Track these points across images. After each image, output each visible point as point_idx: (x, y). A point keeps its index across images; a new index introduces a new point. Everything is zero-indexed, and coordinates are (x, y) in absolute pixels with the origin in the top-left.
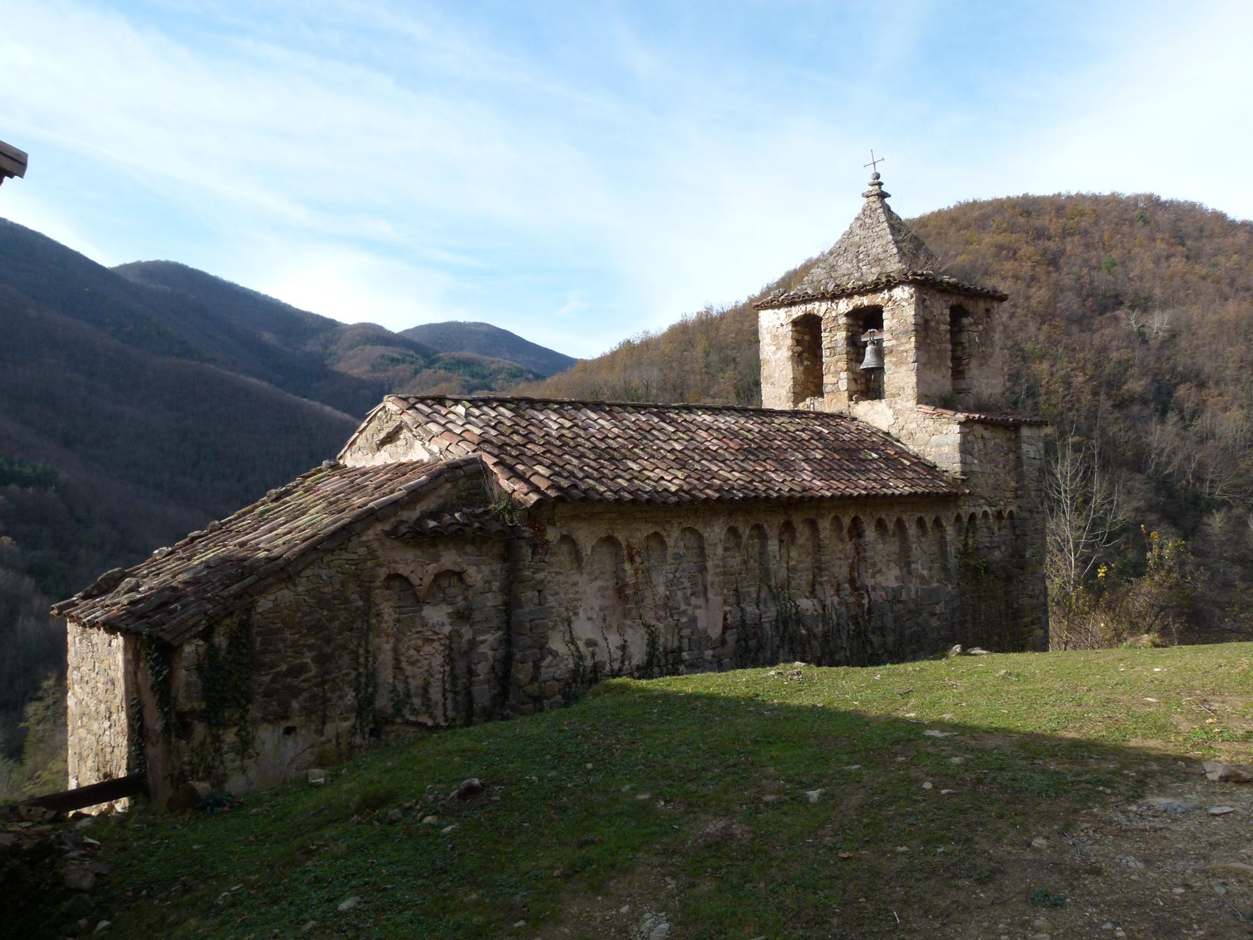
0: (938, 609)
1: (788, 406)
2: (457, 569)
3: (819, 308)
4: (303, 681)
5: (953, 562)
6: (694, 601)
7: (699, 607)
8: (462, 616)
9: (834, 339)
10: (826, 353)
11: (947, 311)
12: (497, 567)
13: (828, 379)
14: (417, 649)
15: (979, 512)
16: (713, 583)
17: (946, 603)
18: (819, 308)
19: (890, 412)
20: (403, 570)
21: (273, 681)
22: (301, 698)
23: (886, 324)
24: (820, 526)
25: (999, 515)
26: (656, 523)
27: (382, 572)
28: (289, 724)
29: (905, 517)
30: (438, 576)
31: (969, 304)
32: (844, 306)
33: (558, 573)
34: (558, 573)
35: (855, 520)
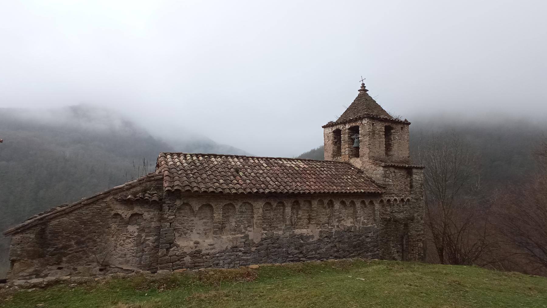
0: (370, 235)
1: (330, 159)
2: (140, 213)
3: (341, 127)
4: (70, 251)
5: (378, 217)
6: (249, 229)
7: (251, 231)
8: (142, 230)
9: (345, 137)
10: (342, 142)
11: (384, 128)
12: (156, 212)
13: (343, 150)
14: (124, 241)
15: (392, 199)
16: (256, 223)
17: (374, 233)
18: (341, 127)
19: (361, 162)
20: (120, 212)
21: (54, 250)
22: (68, 256)
23: (360, 132)
24: (313, 203)
25: (402, 200)
26: (230, 200)
27: (113, 213)
28: (60, 266)
29: (355, 200)
30: (133, 215)
31: (394, 126)
32: (347, 126)
33: (183, 216)
34: (183, 216)
35: (331, 200)
